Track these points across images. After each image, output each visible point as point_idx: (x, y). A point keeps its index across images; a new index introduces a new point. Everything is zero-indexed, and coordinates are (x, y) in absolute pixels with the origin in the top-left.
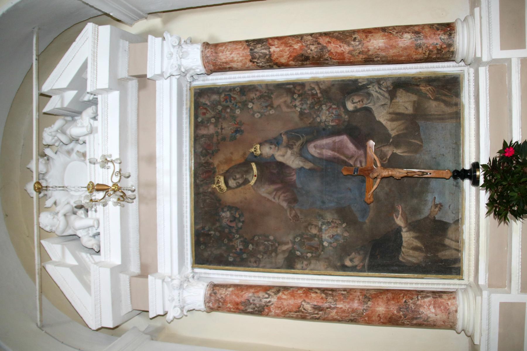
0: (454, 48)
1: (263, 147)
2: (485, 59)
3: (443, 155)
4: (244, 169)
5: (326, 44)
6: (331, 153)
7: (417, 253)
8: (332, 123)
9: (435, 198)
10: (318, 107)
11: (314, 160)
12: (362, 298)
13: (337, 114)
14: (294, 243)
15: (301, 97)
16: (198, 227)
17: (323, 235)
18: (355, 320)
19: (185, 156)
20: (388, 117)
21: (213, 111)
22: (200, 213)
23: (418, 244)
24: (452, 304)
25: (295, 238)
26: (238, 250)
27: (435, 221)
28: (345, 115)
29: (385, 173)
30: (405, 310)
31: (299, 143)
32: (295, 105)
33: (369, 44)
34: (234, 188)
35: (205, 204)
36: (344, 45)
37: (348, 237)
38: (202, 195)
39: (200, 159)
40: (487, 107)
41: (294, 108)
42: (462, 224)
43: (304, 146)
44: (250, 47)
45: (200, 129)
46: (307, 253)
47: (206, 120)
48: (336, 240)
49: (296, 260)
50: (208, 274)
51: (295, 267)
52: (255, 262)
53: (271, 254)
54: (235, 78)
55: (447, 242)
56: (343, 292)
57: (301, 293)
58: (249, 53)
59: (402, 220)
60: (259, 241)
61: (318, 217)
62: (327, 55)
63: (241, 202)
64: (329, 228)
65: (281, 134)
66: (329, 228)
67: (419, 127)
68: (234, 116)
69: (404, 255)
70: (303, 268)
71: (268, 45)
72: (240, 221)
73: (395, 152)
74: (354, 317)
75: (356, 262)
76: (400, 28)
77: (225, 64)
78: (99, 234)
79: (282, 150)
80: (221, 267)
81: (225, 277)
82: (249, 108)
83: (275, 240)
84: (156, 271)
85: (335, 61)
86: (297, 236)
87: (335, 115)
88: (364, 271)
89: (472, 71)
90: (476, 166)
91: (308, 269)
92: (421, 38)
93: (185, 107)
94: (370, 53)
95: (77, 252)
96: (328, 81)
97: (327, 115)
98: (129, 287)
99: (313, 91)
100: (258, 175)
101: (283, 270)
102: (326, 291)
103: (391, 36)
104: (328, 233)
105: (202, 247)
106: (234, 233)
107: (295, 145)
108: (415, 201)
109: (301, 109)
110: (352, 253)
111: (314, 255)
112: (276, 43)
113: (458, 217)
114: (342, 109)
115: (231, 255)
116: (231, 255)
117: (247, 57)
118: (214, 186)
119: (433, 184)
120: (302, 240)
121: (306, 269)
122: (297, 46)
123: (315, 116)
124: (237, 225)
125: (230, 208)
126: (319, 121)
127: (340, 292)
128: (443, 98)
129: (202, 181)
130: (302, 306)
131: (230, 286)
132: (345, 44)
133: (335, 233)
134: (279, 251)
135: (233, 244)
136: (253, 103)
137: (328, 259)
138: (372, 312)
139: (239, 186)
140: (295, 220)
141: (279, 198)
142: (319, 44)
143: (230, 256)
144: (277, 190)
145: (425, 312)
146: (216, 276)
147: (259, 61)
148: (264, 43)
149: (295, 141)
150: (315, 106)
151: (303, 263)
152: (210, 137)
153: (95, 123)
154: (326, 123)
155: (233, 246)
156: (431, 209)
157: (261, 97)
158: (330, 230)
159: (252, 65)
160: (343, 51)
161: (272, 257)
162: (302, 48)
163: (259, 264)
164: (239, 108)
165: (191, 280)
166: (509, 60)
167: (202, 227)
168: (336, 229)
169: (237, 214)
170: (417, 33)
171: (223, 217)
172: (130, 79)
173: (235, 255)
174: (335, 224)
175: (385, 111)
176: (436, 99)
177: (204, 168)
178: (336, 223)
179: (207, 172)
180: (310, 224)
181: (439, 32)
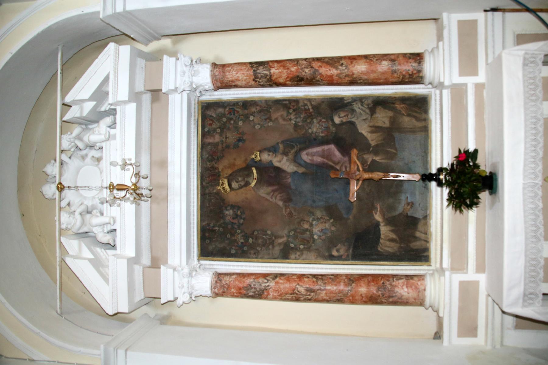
0: (423, 74)
1: (262, 154)
2: (447, 83)
3: (414, 162)
4: (246, 173)
5: (318, 68)
7: (392, 244)
9: (407, 197)
10: (310, 120)
11: (306, 165)
12: (347, 281)
14: (288, 236)
16: (204, 223)
18: (341, 300)
19: (192, 161)
20: (369, 129)
21: (219, 122)
22: (206, 211)
23: (394, 236)
24: (421, 284)
25: (289, 232)
26: (239, 243)
27: (407, 216)
29: (366, 176)
30: (383, 290)
31: (293, 151)
32: (291, 118)
33: (353, 69)
34: (236, 190)
35: (210, 203)
36: (333, 69)
37: (335, 231)
38: (207, 196)
39: (206, 164)
40: (449, 122)
42: (430, 219)
43: (297, 154)
44: (254, 69)
45: (207, 138)
46: (300, 245)
47: (212, 130)
48: (325, 233)
49: (291, 252)
50: (212, 265)
52: (255, 254)
53: (268, 246)
54: (238, 94)
55: (418, 234)
56: (331, 277)
57: (295, 278)
58: (252, 74)
59: (381, 217)
60: (258, 235)
62: (319, 77)
63: (243, 202)
64: (319, 223)
66: (319, 223)
67: (394, 138)
68: (237, 127)
69: (382, 246)
70: (297, 258)
71: (269, 67)
72: (241, 218)
73: (374, 158)
74: (340, 297)
75: (342, 252)
76: (379, 56)
77: (231, 82)
78: (115, 230)
79: (279, 157)
80: (225, 259)
81: (227, 267)
82: (251, 121)
83: (272, 234)
84: (166, 263)
85: (325, 82)
86: (291, 230)
87: (324, 128)
88: (349, 260)
89: (438, 92)
90: (440, 170)
92: (396, 65)
93: (193, 118)
94: (355, 76)
95: (92, 247)
96: (319, 98)
97: (317, 128)
98: (142, 276)
99: (306, 107)
100: (257, 178)
101: (278, 260)
102: (316, 276)
103: (372, 62)
104: (318, 228)
105: (207, 241)
106: (236, 229)
107: (290, 152)
108: (391, 200)
109: (295, 121)
110: (338, 244)
111: (306, 246)
112: (276, 66)
113: (427, 213)
114: (330, 123)
115: (233, 248)
116: (233, 248)
117: (250, 77)
118: (219, 188)
119: (406, 186)
120: (296, 234)
121: (299, 259)
122: (293, 69)
123: (307, 128)
124: (239, 222)
125: (233, 207)
127: (328, 277)
128: (415, 114)
129: (209, 183)
130: (296, 289)
131: (233, 274)
132: (334, 68)
133: (324, 228)
134: (275, 244)
135: (235, 238)
136: (254, 116)
137: (317, 249)
138: (356, 292)
139: (241, 187)
141: (276, 198)
142: (312, 67)
143: (233, 249)
144: (274, 191)
145: (399, 292)
146: (219, 267)
147: (260, 81)
148: (266, 66)
149: (290, 149)
151: (296, 253)
152: (216, 145)
153: (112, 131)
154: (316, 134)
155: (235, 240)
156: (404, 207)
157: (260, 111)
158: (320, 225)
159: (254, 84)
160: (331, 74)
161: (269, 249)
162: (298, 70)
163: (258, 256)
164: (241, 120)
165: (198, 270)
166: (466, 85)
167: (208, 224)
169: (239, 212)
170: (393, 60)
171: (226, 214)
172: (145, 93)
173: (237, 248)
175: (366, 125)
176: (409, 115)
177: (210, 172)
178: (324, 219)
179: (212, 175)
180: (303, 220)
181: (410, 60)
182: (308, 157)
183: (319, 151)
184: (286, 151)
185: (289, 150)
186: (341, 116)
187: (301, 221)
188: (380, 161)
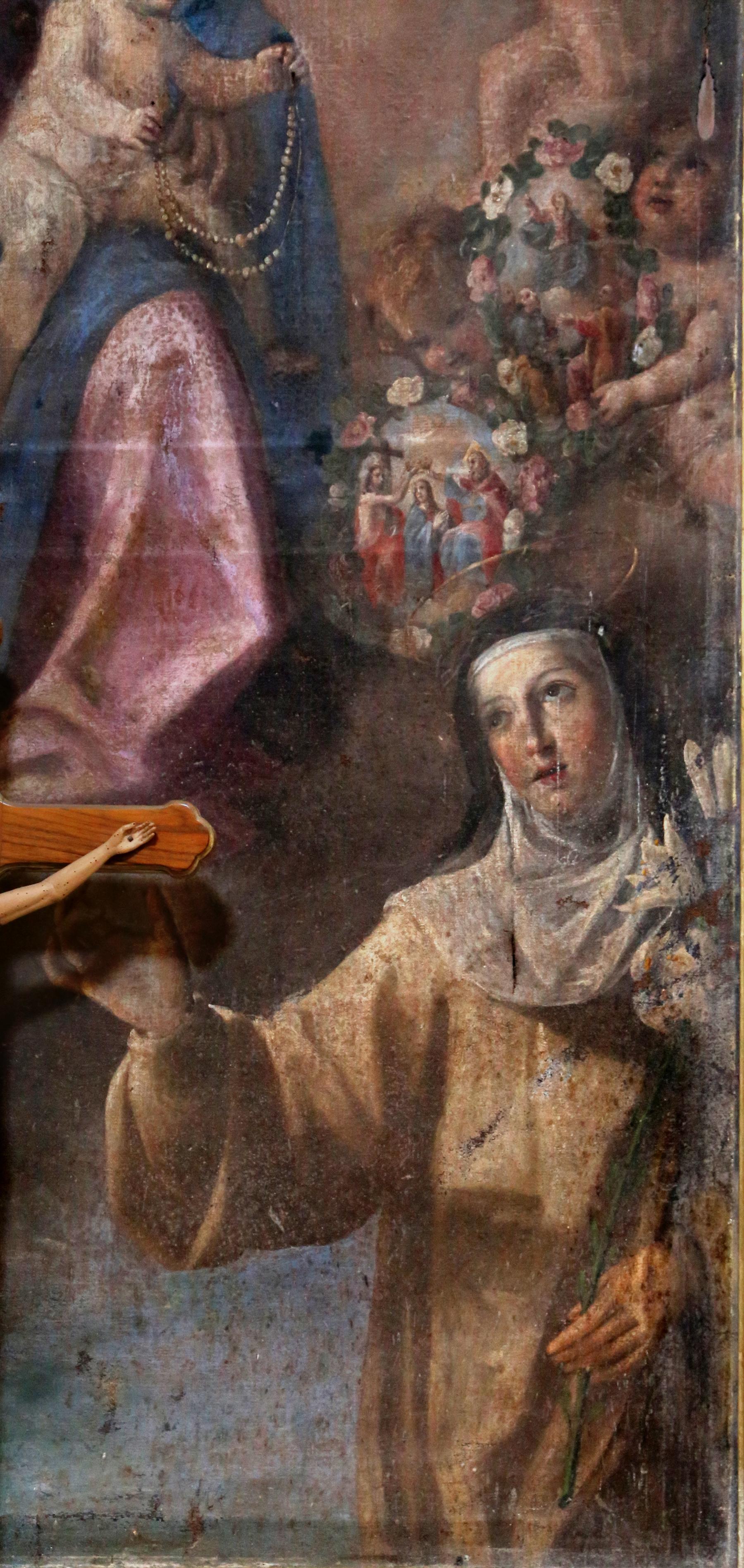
6: (120, 503)
8: (374, 516)
10: (514, 387)
13: (445, 550)
15: (603, 219)
28: (435, 630)
32: (538, 172)
41: (507, 159)
65: (284, 39)
87: (437, 535)
99: (651, 330)
107: (187, 180)
109: (502, 226)
123: (431, 357)
126: (393, 396)
149: (219, 173)
150: (523, 359)
182: (144, 376)
183: (201, 482)
184: (199, 123)
185: (212, 156)
186: (551, 706)
188: (112, 1099)
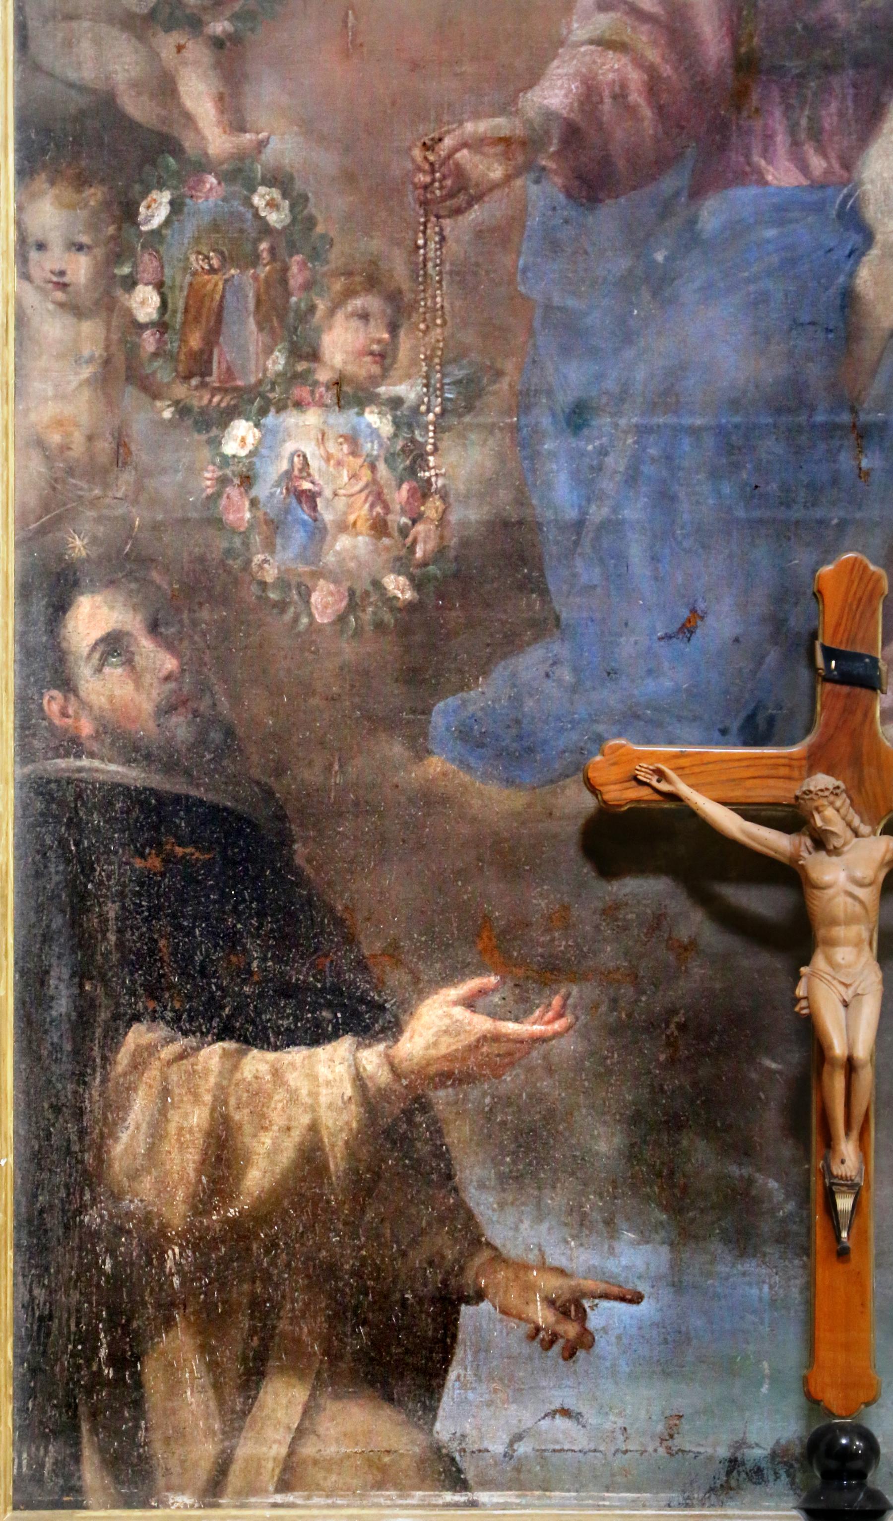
17: (312, 418)
37: (305, 620)
46: (159, 286)
49: (95, 195)
51: (41, 181)
61: (459, 373)
64: (373, 468)
66: (373, 468)
70: (34, 255)
86: (298, 202)
91: (32, 298)
104: (328, 458)
111: (149, 341)
120: (264, 246)
133: (328, 516)
140: (426, 187)
141: (605, 43)
151: (80, 248)
158: (354, 476)
168: (363, 526)
174: (403, 512)
187: (394, 297)
